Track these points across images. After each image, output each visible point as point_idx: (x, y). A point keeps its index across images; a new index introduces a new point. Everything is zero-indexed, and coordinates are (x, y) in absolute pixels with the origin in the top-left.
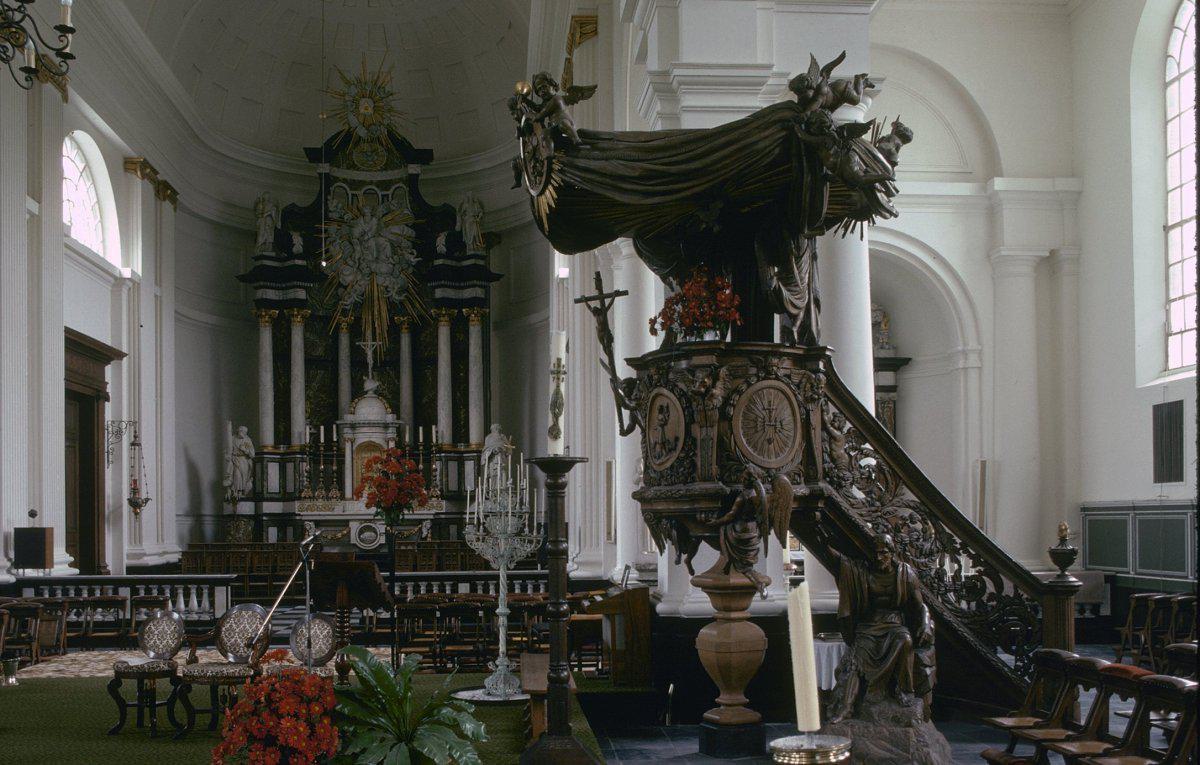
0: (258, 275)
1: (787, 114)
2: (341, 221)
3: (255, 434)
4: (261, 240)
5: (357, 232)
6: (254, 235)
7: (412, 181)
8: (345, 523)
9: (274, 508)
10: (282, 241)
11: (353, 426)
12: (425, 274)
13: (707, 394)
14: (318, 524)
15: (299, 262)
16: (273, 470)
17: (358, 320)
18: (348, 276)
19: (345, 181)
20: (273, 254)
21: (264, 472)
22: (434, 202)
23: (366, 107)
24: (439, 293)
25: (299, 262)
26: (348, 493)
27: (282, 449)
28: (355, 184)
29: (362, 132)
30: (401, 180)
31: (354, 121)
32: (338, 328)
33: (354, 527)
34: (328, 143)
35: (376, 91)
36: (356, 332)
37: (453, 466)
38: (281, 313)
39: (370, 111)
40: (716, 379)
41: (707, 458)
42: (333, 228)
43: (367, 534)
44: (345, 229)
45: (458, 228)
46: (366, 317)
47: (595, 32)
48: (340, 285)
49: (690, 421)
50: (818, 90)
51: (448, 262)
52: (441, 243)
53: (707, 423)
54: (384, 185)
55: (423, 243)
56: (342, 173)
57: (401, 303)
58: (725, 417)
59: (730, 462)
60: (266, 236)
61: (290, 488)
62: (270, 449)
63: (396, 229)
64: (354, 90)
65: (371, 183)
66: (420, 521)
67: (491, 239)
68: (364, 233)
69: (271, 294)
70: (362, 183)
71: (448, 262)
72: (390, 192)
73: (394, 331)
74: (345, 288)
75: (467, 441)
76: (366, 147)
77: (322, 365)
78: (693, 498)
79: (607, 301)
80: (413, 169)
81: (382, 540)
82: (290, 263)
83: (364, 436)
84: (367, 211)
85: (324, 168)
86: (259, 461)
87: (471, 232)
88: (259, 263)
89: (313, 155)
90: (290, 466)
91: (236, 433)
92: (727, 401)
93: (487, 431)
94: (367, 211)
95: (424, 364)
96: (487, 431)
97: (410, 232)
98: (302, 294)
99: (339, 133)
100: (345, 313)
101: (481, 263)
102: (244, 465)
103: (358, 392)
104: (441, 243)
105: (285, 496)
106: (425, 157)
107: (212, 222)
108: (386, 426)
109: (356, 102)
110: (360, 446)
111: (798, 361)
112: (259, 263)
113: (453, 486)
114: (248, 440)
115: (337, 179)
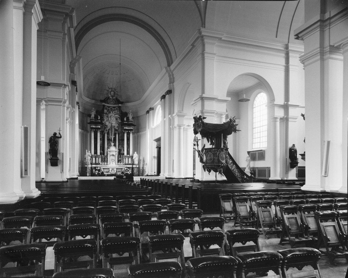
0: (91, 123)
1: (229, 123)
2: (106, 114)
3: (91, 152)
4: (92, 116)
5: (109, 116)
6: (90, 116)
7: (119, 107)
8: (109, 169)
9: (94, 166)
10: (96, 117)
11: (110, 151)
12: (122, 124)
13: (217, 154)
14: (103, 169)
15: (99, 121)
16: (94, 159)
17: (109, 132)
18: (107, 123)
19: (107, 106)
20: (94, 119)
21: (92, 159)
22: (124, 111)
23: (112, 93)
24: (125, 128)
25: (99, 121)
26: (108, 163)
27: (95, 155)
28: (109, 107)
29: (111, 98)
30: (117, 107)
31: (110, 95)
32: (105, 133)
33: (110, 169)
34: (105, 99)
35: (114, 90)
36: (108, 134)
37: (127, 159)
38: (96, 130)
39: (113, 94)
40: (218, 152)
41: (216, 161)
42: (105, 115)
43: (113, 171)
44: (107, 115)
45: (128, 116)
46: (110, 131)
47: (171, 93)
48: (106, 125)
49: (214, 157)
50: (232, 120)
51: (126, 122)
52: (125, 119)
53: (216, 157)
54: (114, 107)
55: (122, 120)
56: (106, 105)
57: (117, 129)
58: (218, 156)
59: (219, 161)
60: (93, 116)
61: (97, 162)
62: (93, 155)
63: (116, 116)
64: (110, 90)
65: (111, 107)
66: (122, 169)
67: (133, 118)
68: (111, 116)
69: (94, 126)
70: (110, 107)
71: (126, 122)
72: (115, 109)
73: (115, 134)
74: (107, 126)
75: (129, 154)
76: (111, 100)
77: (103, 140)
78: (214, 166)
79: (198, 141)
80: (120, 105)
81: (115, 172)
82: (98, 121)
83: (111, 153)
84: (111, 112)
85: (104, 104)
86: (92, 157)
87: (131, 118)
88: (91, 121)
89: (102, 101)
90: (97, 159)
91: (88, 152)
92: (219, 154)
93: (133, 153)
94: (111, 112)
95: (121, 140)
96: (133, 153)
97: (118, 116)
98: (99, 127)
99: (107, 98)
100: (106, 130)
101: (132, 123)
102: (89, 158)
103: (109, 146)
104: (125, 119)
105: (96, 164)
106: (122, 103)
107: (81, 112)
108: (116, 151)
109: (110, 92)
110: (111, 155)
111: (225, 150)
112: (91, 121)
113: (127, 162)
114: (90, 153)
115: (105, 106)
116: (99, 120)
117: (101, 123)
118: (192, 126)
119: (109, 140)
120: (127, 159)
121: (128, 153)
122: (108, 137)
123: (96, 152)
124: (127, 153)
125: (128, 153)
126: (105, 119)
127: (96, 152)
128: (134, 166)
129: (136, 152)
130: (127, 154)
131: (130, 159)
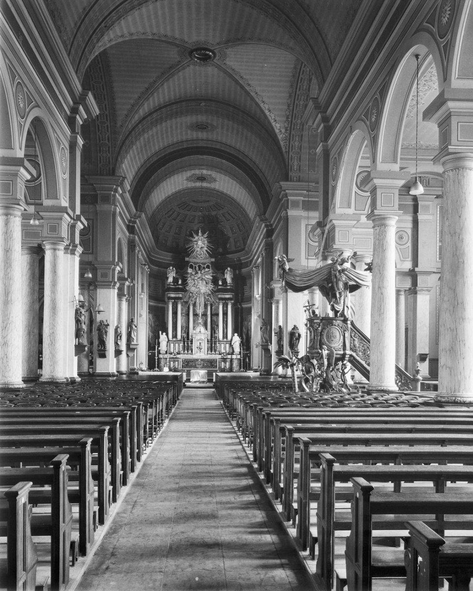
15: (180, 286)
17: (195, 303)
18: (193, 289)
24: (220, 296)
25: (180, 286)
27: (174, 339)
36: (194, 305)
38: (175, 301)
42: (189, 275)
52: (220, 283)
73: (206, 306)
75: (227, 338)
91: (162, 334)
93: (233, 335)
95: (215, 315)
96: (233, 335)
98: (181, 296)
104: (220, 283)
116: (180, 285)
117: (184, 290)
118: (371, 281)
119: (195, 315)
120: (223, 345)
121: (225, 335)
122: (194, 311)
123: (175, 336)
124: (223, 336)
125: (225, 335)
126: (190, 281)
127: (175, 336)
128: (234, 357)
129: (236, 334)
130: (223, 338)
131: (228, 346)
